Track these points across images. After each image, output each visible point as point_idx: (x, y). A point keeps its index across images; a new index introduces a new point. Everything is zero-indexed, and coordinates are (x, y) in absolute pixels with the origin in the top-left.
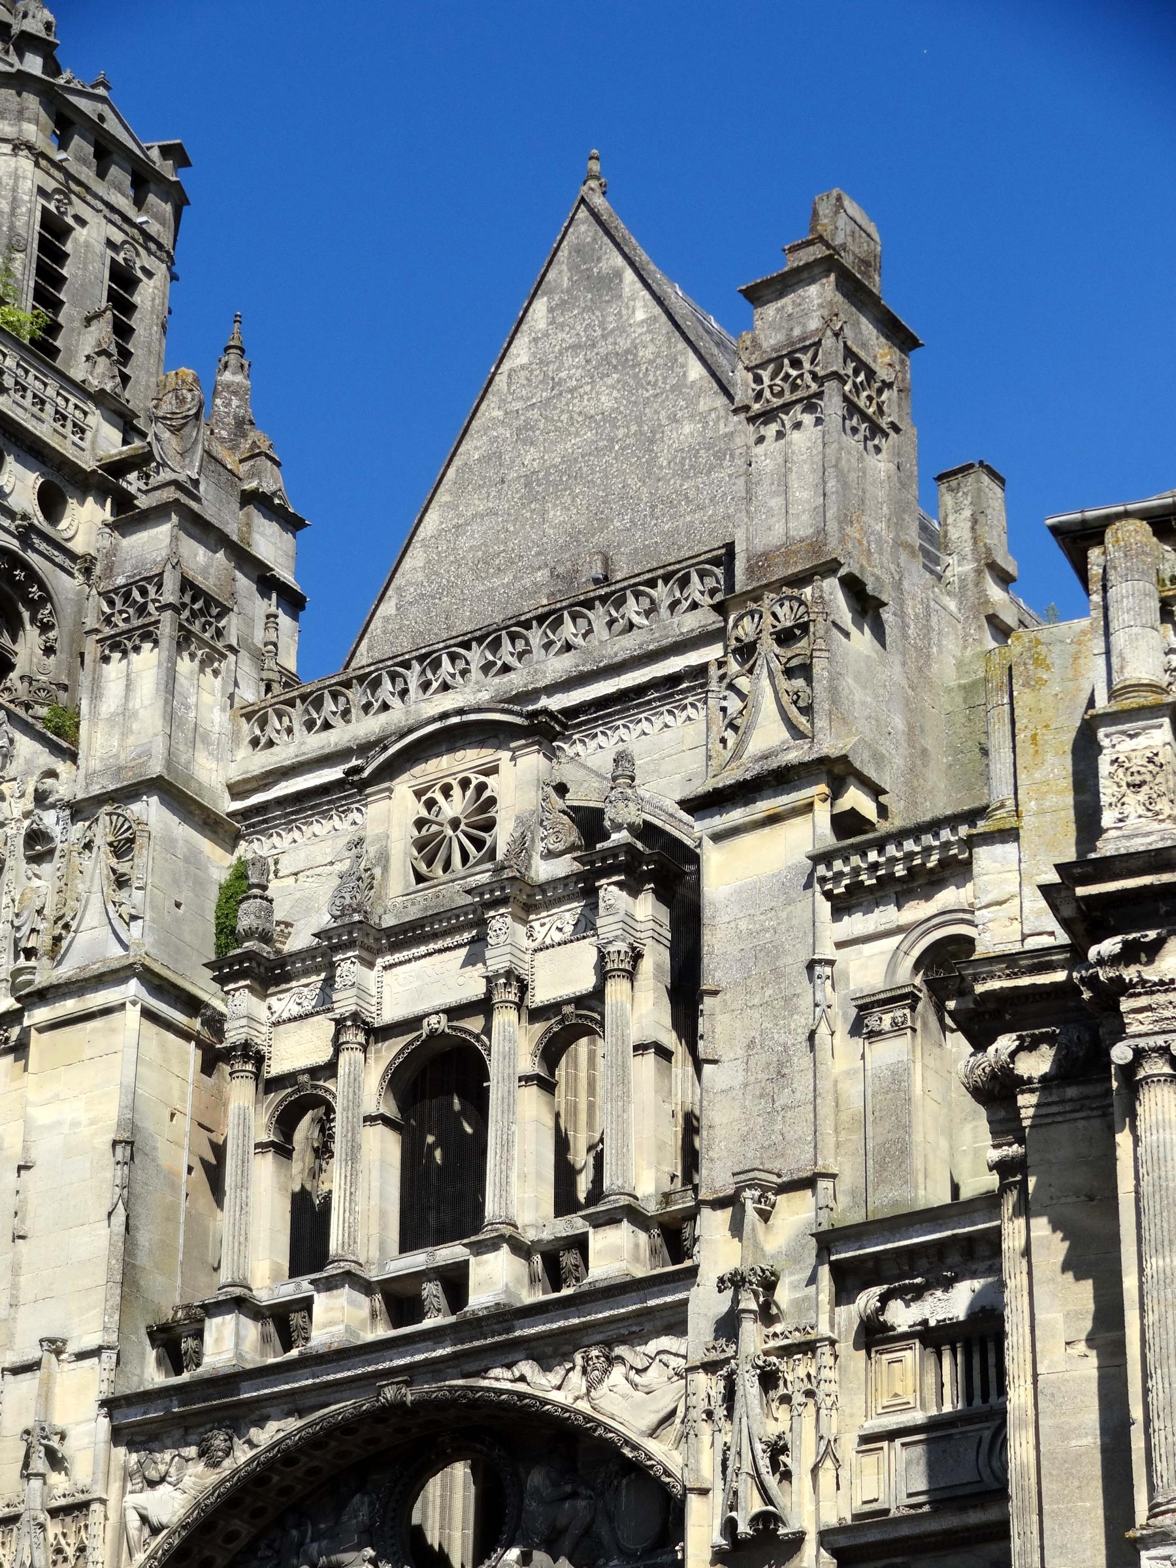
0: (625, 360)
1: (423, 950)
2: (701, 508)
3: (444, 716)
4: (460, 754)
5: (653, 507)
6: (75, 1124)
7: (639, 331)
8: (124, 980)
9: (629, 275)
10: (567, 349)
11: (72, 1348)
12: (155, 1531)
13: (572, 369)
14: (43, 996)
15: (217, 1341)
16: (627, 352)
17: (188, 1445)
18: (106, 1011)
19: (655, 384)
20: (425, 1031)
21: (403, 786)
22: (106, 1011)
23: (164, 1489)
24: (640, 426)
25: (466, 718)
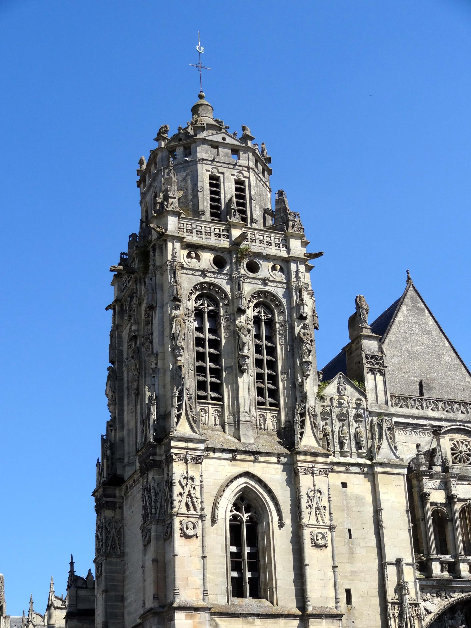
0: (429, 332)
1: (465, 483)
2: (453, 379)
3: (460, 425)
4: (460, 435)
5: (442, 374)
6: (393, 502)
7: (431, 327)
8: (404, 468)
9: (426, 311)
10: (414, 322)
11: (404, 562)
12: (429, 612)
13: (415, 328)
14: (381, 464)
15: (436, 568)
16: (429, 331)
17: (434, 593)
18: (398, 474)
19: (438, 343)
20: (468, 503)
21: (447, 437)
22: (398, 474)
23: (427, 602)
24: (435, 351)
25: (465, 428)
